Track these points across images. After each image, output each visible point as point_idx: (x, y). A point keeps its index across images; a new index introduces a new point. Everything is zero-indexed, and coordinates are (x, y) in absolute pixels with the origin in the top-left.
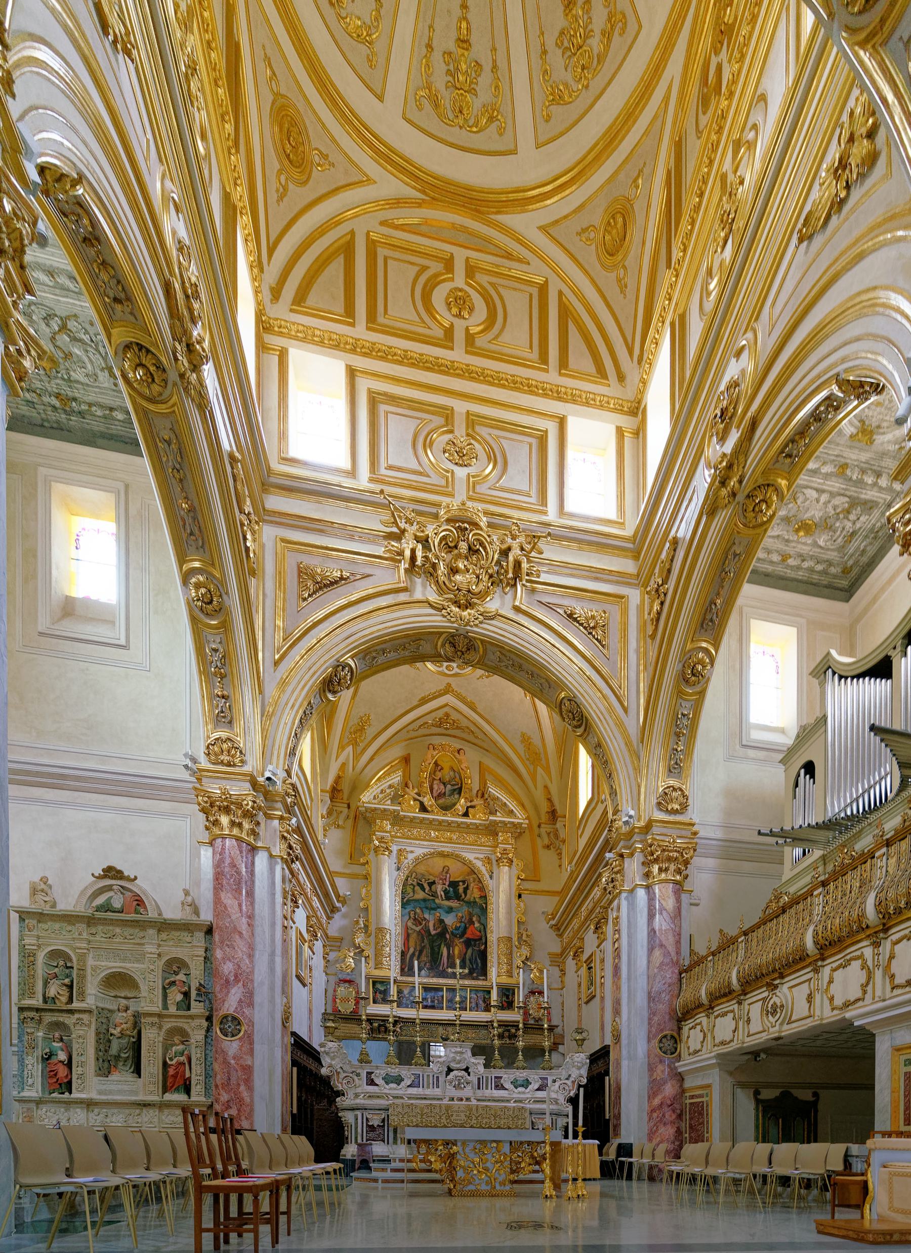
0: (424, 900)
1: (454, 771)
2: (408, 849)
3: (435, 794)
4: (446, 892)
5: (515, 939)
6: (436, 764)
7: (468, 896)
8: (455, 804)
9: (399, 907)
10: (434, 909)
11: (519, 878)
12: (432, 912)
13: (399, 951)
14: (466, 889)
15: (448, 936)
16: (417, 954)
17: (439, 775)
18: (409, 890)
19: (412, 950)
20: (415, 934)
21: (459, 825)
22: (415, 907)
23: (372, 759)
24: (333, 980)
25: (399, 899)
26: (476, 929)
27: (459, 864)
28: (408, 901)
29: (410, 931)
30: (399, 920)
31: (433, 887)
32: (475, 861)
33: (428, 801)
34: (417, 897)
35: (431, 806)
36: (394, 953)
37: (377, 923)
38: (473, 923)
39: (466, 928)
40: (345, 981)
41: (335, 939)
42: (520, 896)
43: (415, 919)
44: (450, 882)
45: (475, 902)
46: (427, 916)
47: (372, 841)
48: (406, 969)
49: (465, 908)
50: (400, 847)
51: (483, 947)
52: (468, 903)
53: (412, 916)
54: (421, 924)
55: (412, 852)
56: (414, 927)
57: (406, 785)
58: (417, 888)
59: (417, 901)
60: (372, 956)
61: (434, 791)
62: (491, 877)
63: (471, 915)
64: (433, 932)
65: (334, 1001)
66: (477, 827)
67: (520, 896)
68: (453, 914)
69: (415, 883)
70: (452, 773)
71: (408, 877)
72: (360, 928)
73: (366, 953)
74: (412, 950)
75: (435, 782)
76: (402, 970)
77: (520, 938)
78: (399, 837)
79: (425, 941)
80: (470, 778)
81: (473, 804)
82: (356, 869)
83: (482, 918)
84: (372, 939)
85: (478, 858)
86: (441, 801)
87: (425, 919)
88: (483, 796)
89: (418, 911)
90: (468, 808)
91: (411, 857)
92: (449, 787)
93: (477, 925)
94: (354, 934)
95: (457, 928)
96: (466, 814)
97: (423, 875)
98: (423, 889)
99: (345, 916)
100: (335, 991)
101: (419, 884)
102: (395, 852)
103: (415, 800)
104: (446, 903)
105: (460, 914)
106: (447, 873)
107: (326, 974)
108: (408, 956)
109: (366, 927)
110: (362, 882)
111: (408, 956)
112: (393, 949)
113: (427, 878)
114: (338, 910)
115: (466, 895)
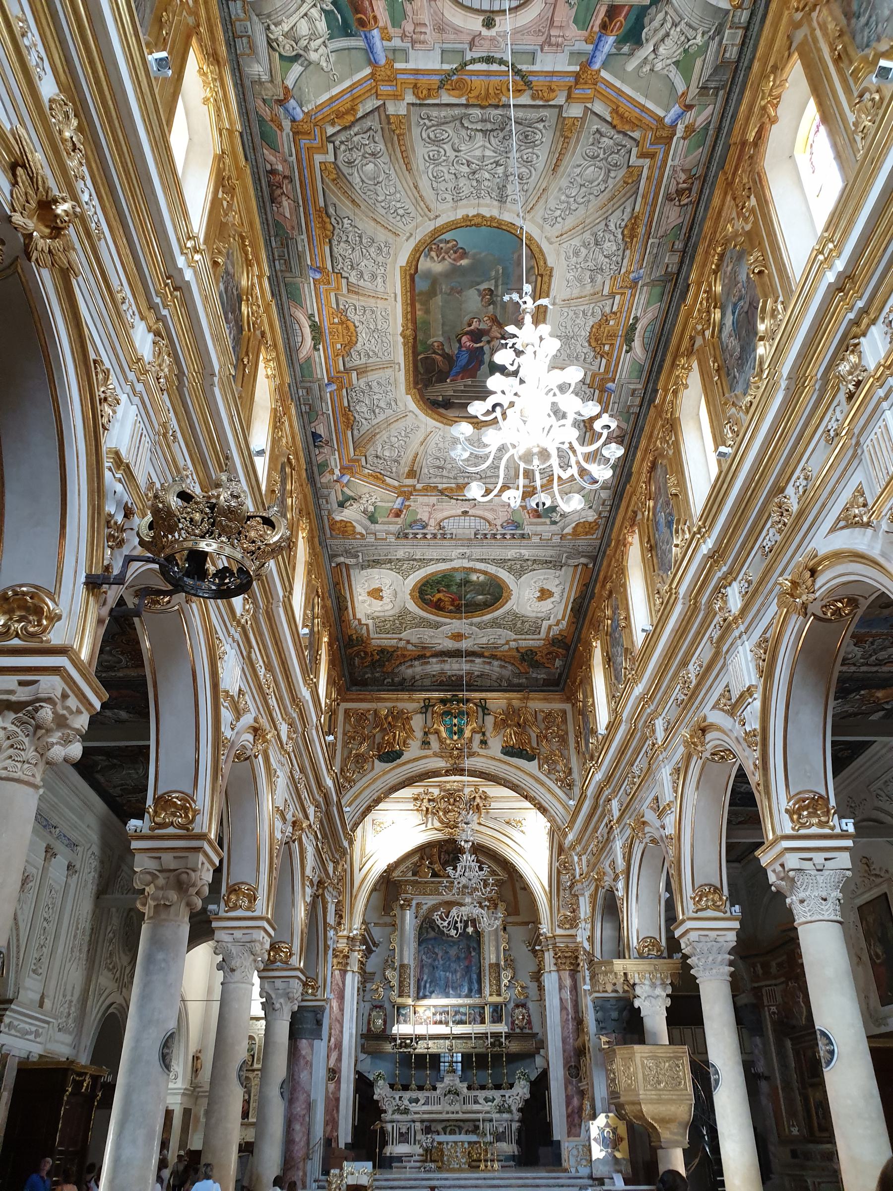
2: (424, 902)
19: (425, 978)
24: (368, 1006)
33: (437, 867)
40: (376, 1007)
47: (398, 900)
48: (421, 994)
58: (429, 930)
59: (430, 939)
63: (469, 947)
65: (369, 1023)
67: (505, 929)
68: (456, 947)
76: (418, 993)
82: (387, 919)
91: (425, 907)
93: (473, 954)
94: (384, 970)
100: (370, 1015)
101: (430, 927)
110: (390, 929)
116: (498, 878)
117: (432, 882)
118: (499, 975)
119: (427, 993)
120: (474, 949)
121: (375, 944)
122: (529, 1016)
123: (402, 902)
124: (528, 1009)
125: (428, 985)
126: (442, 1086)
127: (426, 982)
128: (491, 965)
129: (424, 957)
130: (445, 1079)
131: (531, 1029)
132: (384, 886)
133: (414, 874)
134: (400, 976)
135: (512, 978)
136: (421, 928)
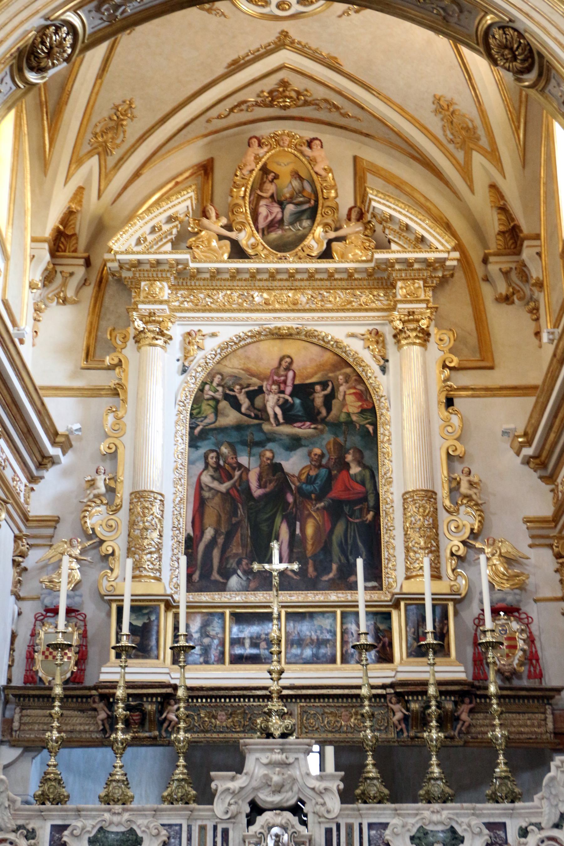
0: (239, 427)
1: (301, 179)
2: (206, 330)
3: (262, 224)
4: (285, 407)
5: (443, 493)
6: (265, 170)
7: (334, 412)
8: (303, 238)
9: (183, 445)
10: (261, 444)
11: (445, 366)
12: (256, 450)
13: (182, 538)
14: (328, 400)
15: (290, 499)
16: (221, 540)
17: (270, 188)
18: (207, 409)
19: (209, 533)
20: (217, 500)
21: (311, 276)
22: (219, 444)
23: (137, 174)
25: (184, 430)
26: (353, 478)
27: (315, 350)
28: (204, 434)
29: (206, 494)
30: (184, 472)
31: (258, 401)
32: (346, 342)
34: (224, 421)
35: (254, 247)
36: (168, 543)
37: (135, 482)
38: (347, 466)
39: (330, 478)
41: (43, 522)
42: (450, 402)
43: (218, 468)
44: (295, 387)
45: (350, 423)
46: (243, 460)
47: (129, 321)
49: (328, 438)
50: (188, 329)
51: (370, 516)
52: (336, 426)
53: (212, 461)
54: (230, 477)
55: (213, 335)
56: (215, 485)
57: (205, 214)
58: (224, 404)
59: (223, 430)
60: (121, 552)
61: (261, 219)
62: (384, 370)
63: (341, 450)
64: (257, 492)
65: (30, 658)
66: (350, 276)
67: (450, 402)
69: (218, 396)
70: (296, 184)
71: (204, 384)
72: (97, 496)
73: (106, 548)
74: (209, 533)
75: (262, 202)
77: (454, 490)
78: (188, 310)
79: (240, 512)
80: (334, 187)
81: (340, 233)
83: (367, 454)
84: (123, 516)
85: (353, 335)
86: (274, 235)
87: (240, 466)
88: (360, 216)
89: (225, 450)
90: (330, 242)
91: (211, 345)
92: (290, 208)
93: (355, 470)
94: (85, 509)
95: (310, 480)
96: (327, 254)
97: (236, 379)
98: (236, 405)
99: (66, 473)
100: (34, 634)
101: (226, 397)
102: (177, 338)
103: (221, 237)
104: (287, 429)
105: (317, 451)
106: (288, 369)
107: (18, 598)
108: (201, 547)
109: (111, 490)
111: (201, 547)
112: (168, 533)
113: (244, 382)
114: (53, 461)
115: (329, 410)
116: (431, 256)
117: (235, 275)
118: (435, 526)
119: (216, 576)
120: (360, 463)
121: (53, 434)
122: (531, 640)
123: (139, 324)
124: (527, 622)
125: (216, 554)
126: (232, 785)
127: (213, 542)
128: (406, 497)
129: (206, 479)
130: (250, 763)
131: (540, 676)
132: (89, 291)
133: (176, 244)
134: (132, 524)
135: (474, 535)
136: (198, 400)
